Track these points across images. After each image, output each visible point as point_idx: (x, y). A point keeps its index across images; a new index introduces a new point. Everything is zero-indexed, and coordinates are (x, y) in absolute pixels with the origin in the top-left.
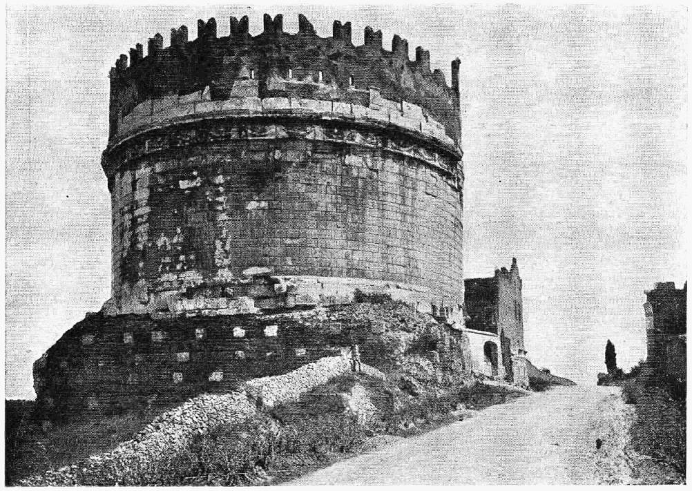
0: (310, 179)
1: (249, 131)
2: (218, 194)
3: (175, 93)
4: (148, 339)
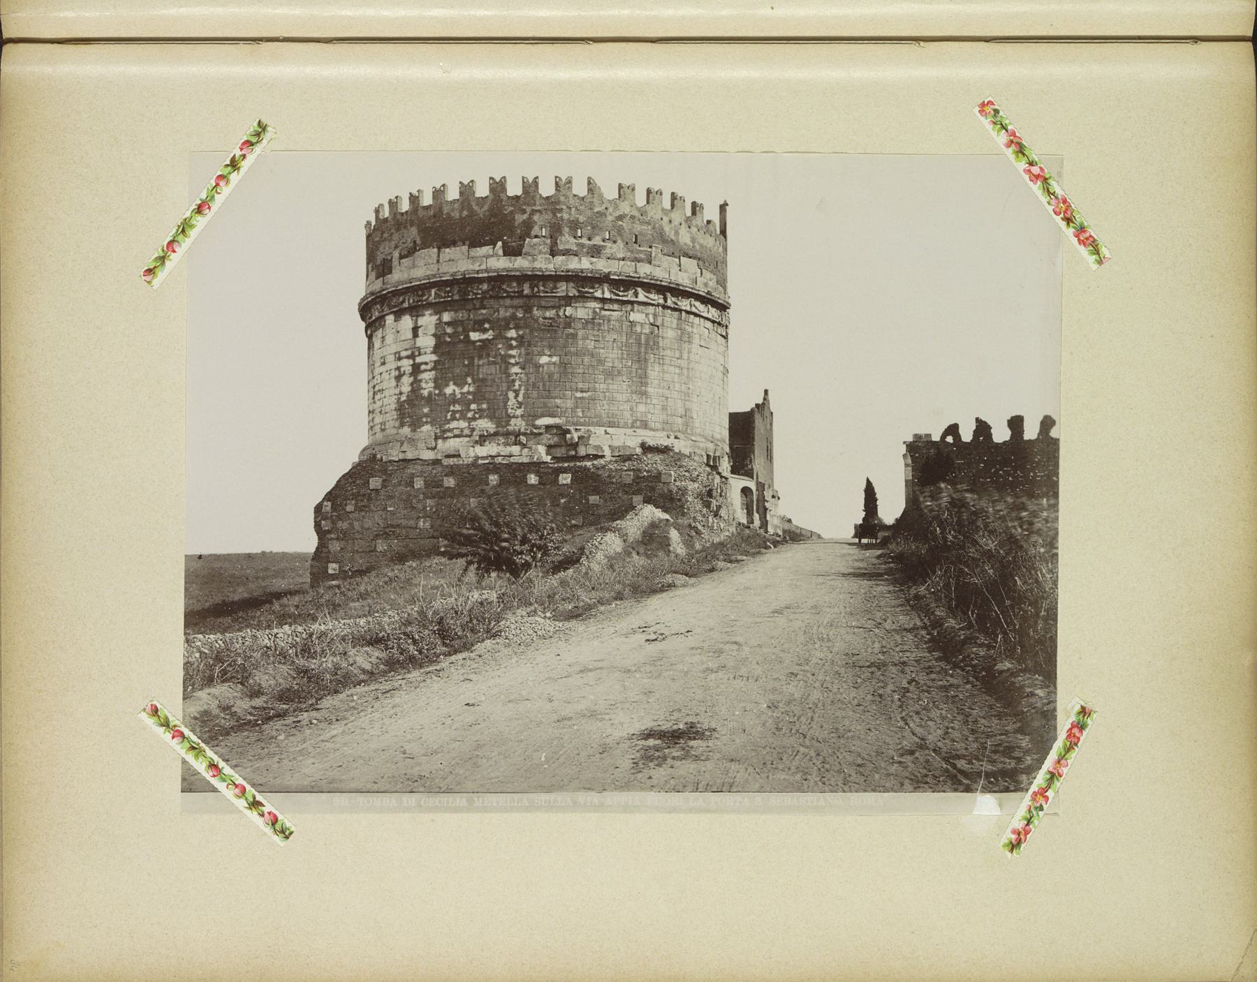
0: (599, 335)
1: (542, 288)
2: (511, 347)
3: (464, 244)
4: (439, 484)
